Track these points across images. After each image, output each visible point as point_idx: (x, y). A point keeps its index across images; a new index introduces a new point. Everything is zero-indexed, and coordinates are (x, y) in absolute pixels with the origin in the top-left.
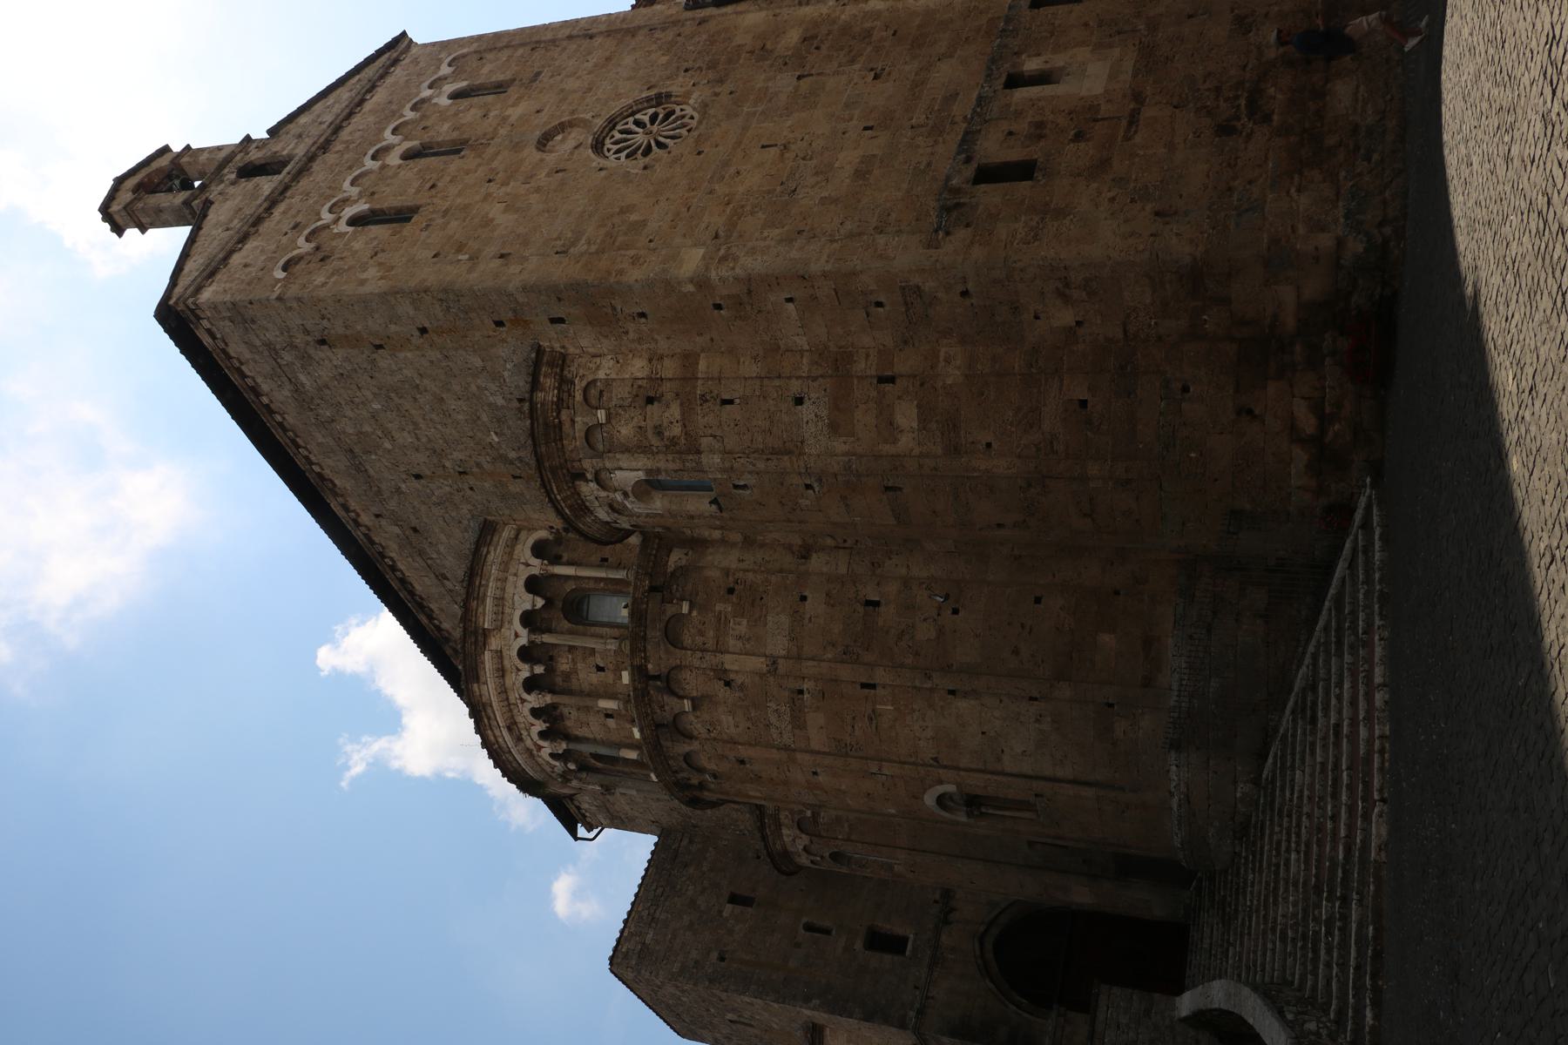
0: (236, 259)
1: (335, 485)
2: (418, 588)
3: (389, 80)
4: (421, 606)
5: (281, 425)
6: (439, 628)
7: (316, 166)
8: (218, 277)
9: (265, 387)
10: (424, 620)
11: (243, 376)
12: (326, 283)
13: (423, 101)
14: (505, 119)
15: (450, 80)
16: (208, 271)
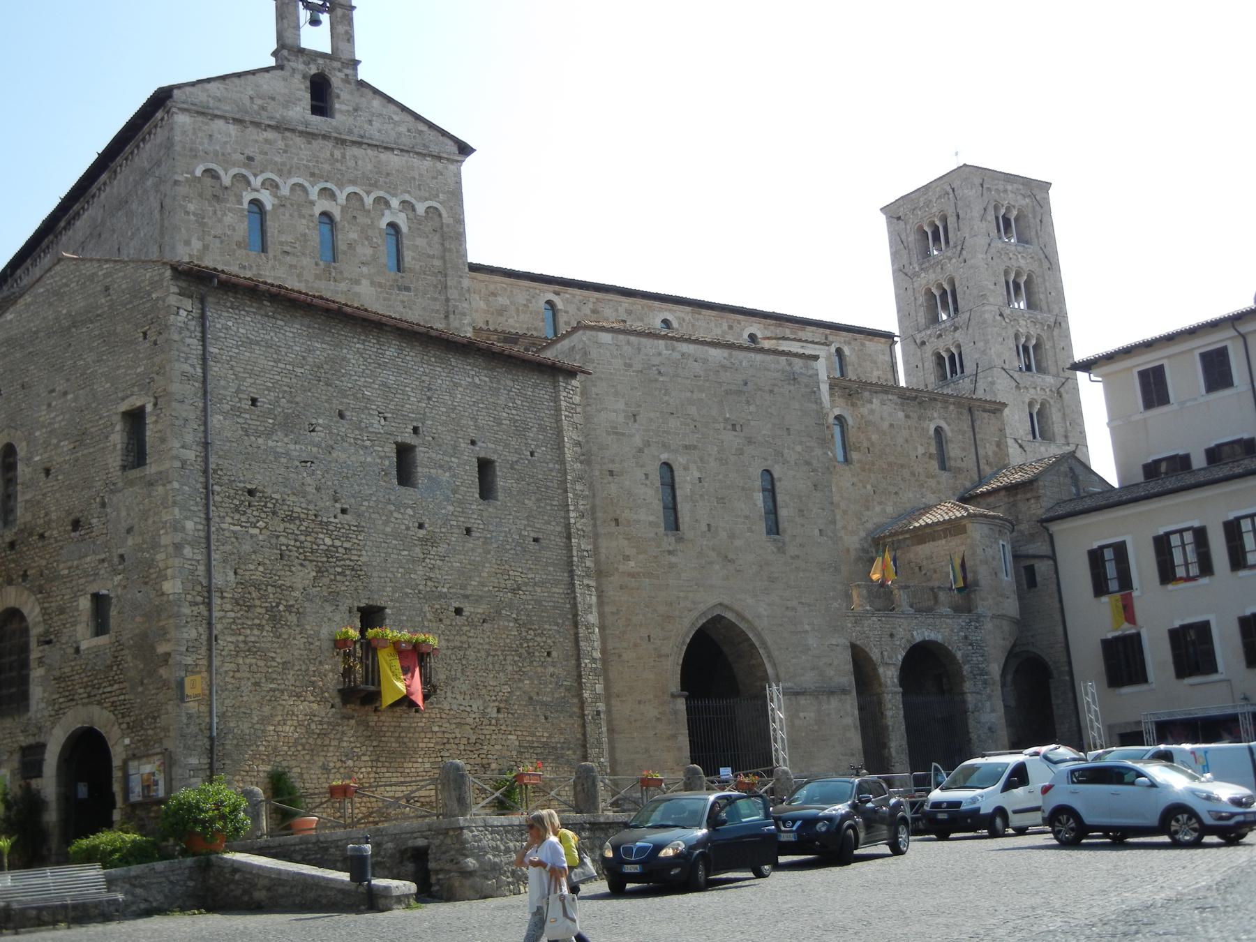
0: (221, 123)
1: (115, 179)
2: (78, 223)
3: (416, 161)
4: (69, 223)
5: (132, 153)
6: (60, 233)
7: (317, 144)
8: (200, 119)
9: (148, 146)
10: (62, 224)
11: (150, 133)
12: (187, 213)
13: (387, 204)
14: (357, 282)
15: (411, 215)
16: (203, 110)
